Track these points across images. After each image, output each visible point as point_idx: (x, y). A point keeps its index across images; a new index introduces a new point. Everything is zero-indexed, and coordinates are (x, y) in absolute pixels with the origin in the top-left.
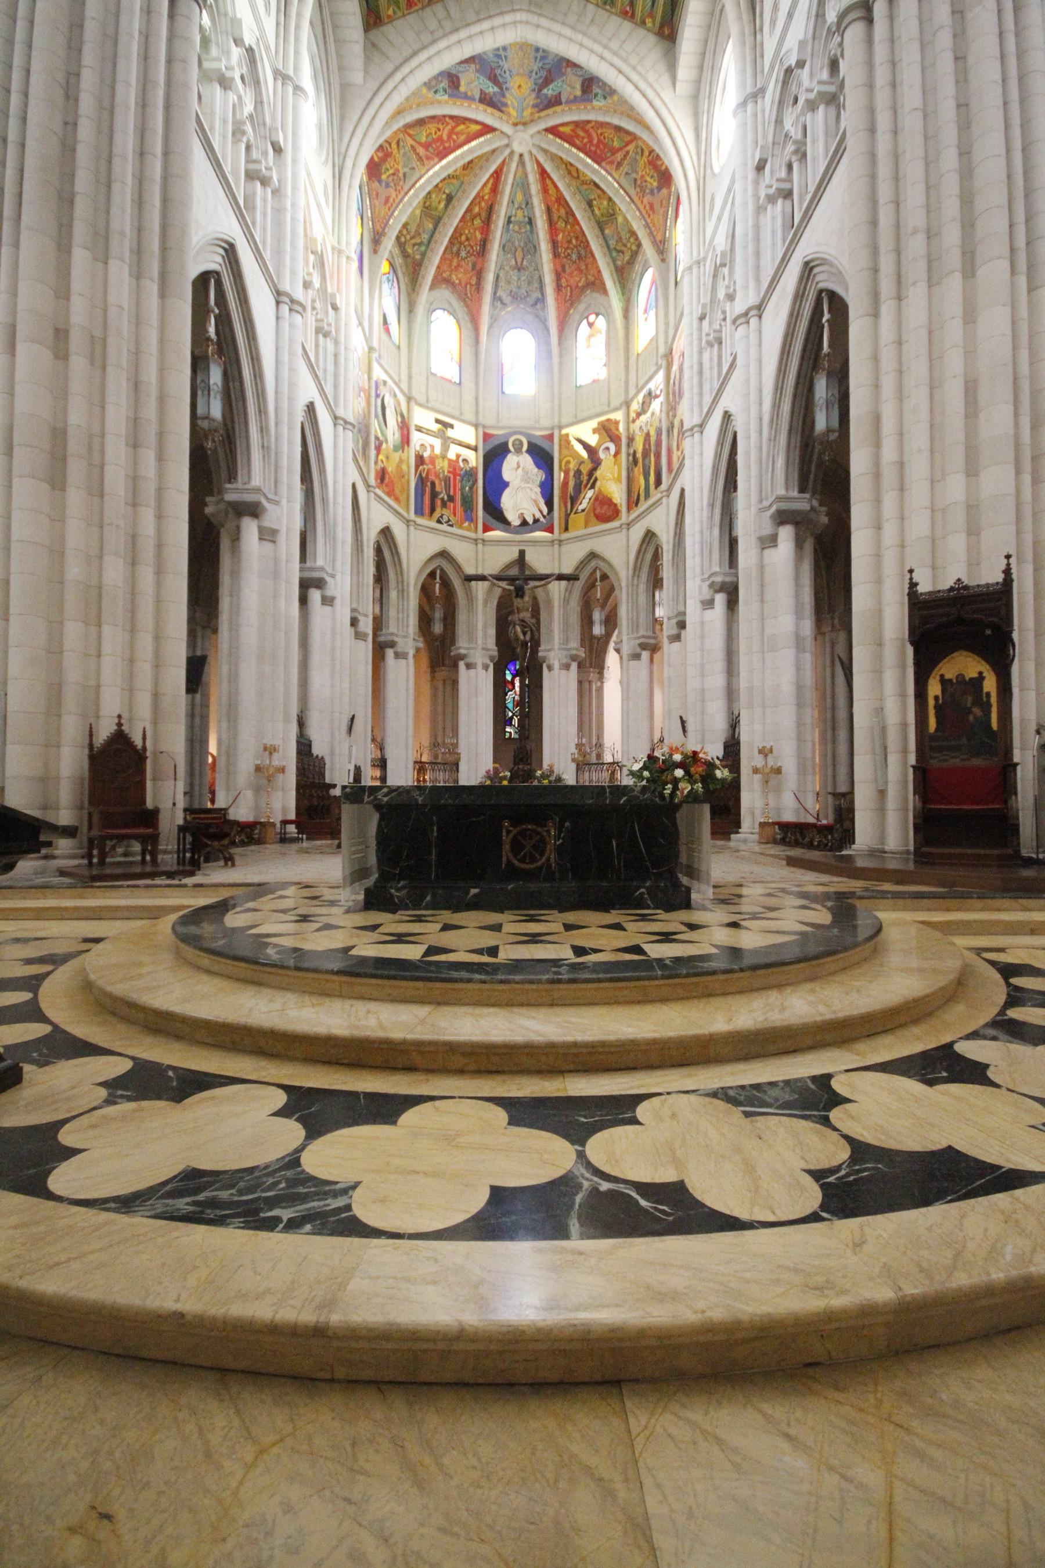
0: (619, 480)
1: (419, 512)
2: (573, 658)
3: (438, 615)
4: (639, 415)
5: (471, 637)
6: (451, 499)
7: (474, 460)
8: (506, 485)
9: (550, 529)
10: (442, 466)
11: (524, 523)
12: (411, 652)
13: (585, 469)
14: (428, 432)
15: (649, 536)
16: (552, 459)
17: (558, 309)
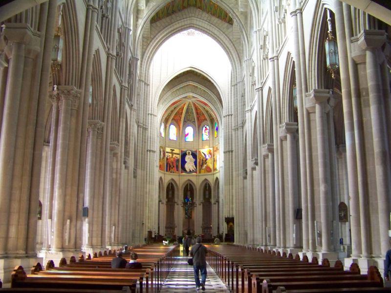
0: (211, 163)
1: (167, 171)
2: (202, 203)
3: (170, 193)
4: (216, 151)
5: (178, 198)
6: (174, 167)
7: (179, 157)
8: (186, 162)
9: (196, 172)
10: (172, 159)
11: (190, 171)
12: (165, 202)
13: (204, 160)
14: (169, 153)
15: (217, 178)
16: (197, 156)
17: (198, 124)
